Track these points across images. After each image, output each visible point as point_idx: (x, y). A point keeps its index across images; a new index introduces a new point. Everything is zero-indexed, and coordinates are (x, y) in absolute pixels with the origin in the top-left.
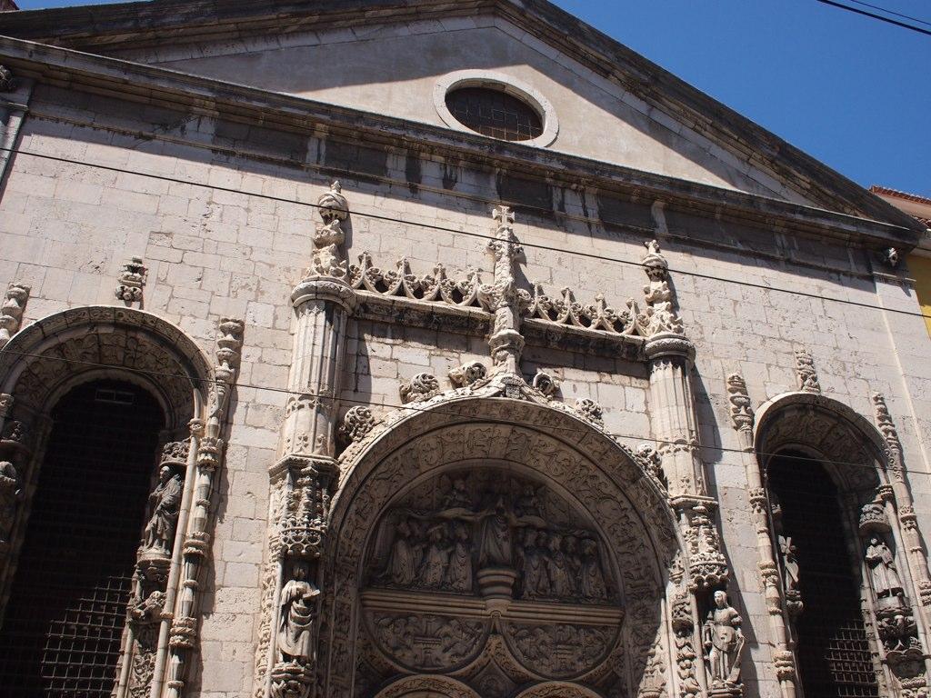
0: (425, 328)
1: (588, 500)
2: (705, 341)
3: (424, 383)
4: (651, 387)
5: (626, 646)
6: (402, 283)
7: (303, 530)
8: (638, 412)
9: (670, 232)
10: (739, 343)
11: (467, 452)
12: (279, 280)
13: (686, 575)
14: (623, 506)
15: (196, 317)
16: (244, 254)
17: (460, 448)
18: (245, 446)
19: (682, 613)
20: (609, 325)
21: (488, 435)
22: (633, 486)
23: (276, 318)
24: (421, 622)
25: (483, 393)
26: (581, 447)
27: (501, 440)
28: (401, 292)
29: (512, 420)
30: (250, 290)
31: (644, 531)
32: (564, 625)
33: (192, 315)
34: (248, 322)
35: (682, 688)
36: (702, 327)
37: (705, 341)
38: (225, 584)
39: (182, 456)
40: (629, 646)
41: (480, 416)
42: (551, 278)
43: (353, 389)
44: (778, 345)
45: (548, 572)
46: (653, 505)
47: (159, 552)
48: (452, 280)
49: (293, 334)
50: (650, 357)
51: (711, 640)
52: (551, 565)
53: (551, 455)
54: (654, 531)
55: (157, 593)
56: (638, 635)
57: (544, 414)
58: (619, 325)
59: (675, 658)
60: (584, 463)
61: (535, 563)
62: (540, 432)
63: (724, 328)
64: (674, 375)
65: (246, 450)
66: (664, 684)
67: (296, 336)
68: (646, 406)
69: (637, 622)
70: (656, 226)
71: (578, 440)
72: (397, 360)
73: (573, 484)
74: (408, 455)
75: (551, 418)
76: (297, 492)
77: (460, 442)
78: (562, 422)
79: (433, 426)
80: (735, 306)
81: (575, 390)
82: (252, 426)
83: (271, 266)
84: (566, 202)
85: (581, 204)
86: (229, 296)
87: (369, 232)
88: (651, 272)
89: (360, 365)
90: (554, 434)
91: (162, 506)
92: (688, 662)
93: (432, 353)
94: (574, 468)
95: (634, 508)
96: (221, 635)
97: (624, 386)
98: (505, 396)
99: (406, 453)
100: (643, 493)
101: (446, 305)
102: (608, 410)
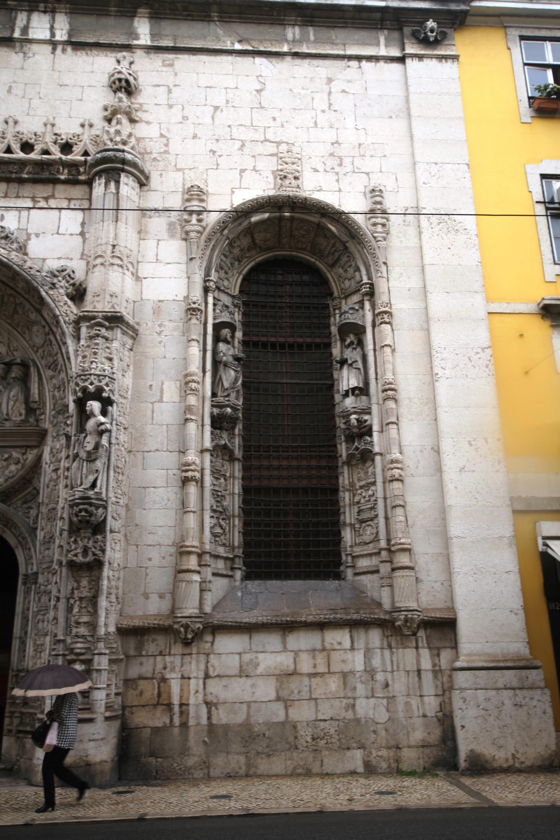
2: (169, 153)
5: (44, 464)
8: (72, 235)
9: (152, 41)
10: (211, 151)
36: (168, 140)
37: (169, 153)
44: (260, 148)
58: (67, 148)
63: (195, 137)
64: (105, 190)
70: (137, 38)
80: (215, 112)
84: (31, 25)
85: (48, 26)
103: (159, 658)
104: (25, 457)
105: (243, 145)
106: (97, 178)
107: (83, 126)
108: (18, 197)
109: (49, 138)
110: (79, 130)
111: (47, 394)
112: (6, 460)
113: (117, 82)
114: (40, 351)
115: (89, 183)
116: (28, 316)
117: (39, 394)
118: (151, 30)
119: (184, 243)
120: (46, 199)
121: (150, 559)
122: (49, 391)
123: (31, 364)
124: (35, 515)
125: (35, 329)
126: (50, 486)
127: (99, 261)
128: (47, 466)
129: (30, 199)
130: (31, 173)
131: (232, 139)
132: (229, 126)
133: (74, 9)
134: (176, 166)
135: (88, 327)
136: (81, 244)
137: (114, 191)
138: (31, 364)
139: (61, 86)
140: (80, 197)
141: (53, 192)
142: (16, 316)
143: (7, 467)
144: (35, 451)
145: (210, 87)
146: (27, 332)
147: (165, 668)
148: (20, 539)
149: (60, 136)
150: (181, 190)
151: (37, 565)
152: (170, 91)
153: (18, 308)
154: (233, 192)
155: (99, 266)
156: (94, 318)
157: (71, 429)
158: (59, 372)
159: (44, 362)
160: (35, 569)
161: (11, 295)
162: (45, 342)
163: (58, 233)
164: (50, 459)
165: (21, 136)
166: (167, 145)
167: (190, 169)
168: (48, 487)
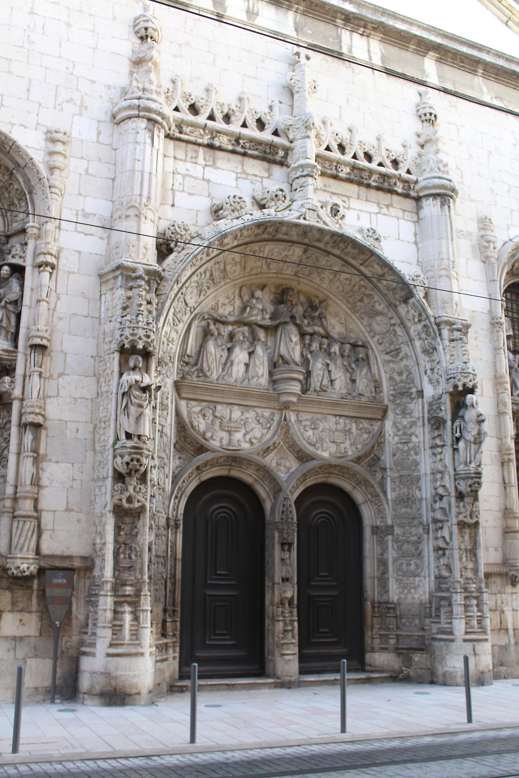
0: (233, 152)
1: (363, 316)
3: (235, 203)
4: (420, 221)
5: (387, 436)
6: (212, 109)
7: (138, 328)
10: (490, 189)
11: (265, 267)
12: (101, 97)
13: (443, 380)
14: (393, 322)
15: (25, 127)
16: (67, 68)
17: (259, 264)
18: (77, 251)
19: (438, 411)
20: (388, 163)
22: (403, 305)
23: (99, 133)
24: (226, 410)
25: (290, 216)
26: (362, 268)
28: (211, 118)
29: (306, 241)
30: (75, 104)
31: (409, 343)
32: (340, 416)
33: (22, 125)
34: (75, 134)
35: (432, 469)
36: (462, 172)
38: (66, 373)
39: (21, 257)
40: (390, 435)
41: (280, 236)
42: (340, 116)
43: (171, 204)
45: (329, 371)
46: (420, 321)
47: (6, 343)
48: (257, 111)
49: (115, 150)
50: (421, 194)
51: (461, 432)
52: (332, 367)
54: (418, 344)
55: (7, 379)
56: (397, 427)
57: (335, 238)
58: (395, 163)
59: (427, 446)
60: (362, 283)
61: (319, 365)
62: (329, 253)
63: (479, 174)
65: (77, 255)
66: (416, 466)
67: (118, 151)
68: (416, 237)
69: (398, 416)
71: (361, 262)
72: (209, 181)
73: (351, 300)
75: (341, 241)
76: (130, 294)
81: (358, 218)
82: (82, 233)
83: (93, 82)
84: (353, 45)
86: (55, 108)
87: (181, 56)
88: (423, 118)
89: (175, 180)
90: (342, 255)
91: (6, 302)
92: (439, 450)
93: (239, 175)
95: (402, 324)
96: (66, 416)
97: (398, 219)
98: (305, 219)
100: (412, 312)
101: (253, 132)
102: (385, 238)
103: (498, 596)
104: (373, 428)
105: (509, 190)
106: (431, 199)
107: (404, 146)
108: (367, 200)
109: (384, 153)
110: (401, 150)
111: (383, 375)
112: (361, 429)
113: (428, 115)
114: (377, 337)
115: (418, 199)
116: (373, 306)
118: (438, 73)
119: (482, 264)
120: (388, 206)
121: (487, 521)
122: (385, 372)
124: (380, 477)
125: (379, 318)
126: (398, 455)
127: (443, 272)
128: (391, 438)
129: (375, 205)
130: (376, 182)
131: (502, 182)
132: (500, 170)
133: (384, 39)
134: (469, 196)
135: (449, 330)
136: (416, 252)
137: (448, 214)
139: (384, 106)
140: (410, 210)
141: (392, 202)
142: (359, 304)
143: (361, 435)
144: (379, 423)
145: (484, 133)
146: (366, 319)
147: (502, 603)
148: (369, 496)
149: (391, 152)
150: (476, 218)
151: (392, 520)
152: (458, 131)
153: (365, 298)
154: (509, 228)
155: (444, 277)
156: (453, 324)
157: (446, 414)
158: (402, 360)
159: (381, 348)
160: (390, 522)
161: (363, 286)
162: (388, 331)
163: (399, 239)
164: (394, 433)
165: (363, 146)
166: (462, 177)
167: (479, 202)
168: (394, 455)
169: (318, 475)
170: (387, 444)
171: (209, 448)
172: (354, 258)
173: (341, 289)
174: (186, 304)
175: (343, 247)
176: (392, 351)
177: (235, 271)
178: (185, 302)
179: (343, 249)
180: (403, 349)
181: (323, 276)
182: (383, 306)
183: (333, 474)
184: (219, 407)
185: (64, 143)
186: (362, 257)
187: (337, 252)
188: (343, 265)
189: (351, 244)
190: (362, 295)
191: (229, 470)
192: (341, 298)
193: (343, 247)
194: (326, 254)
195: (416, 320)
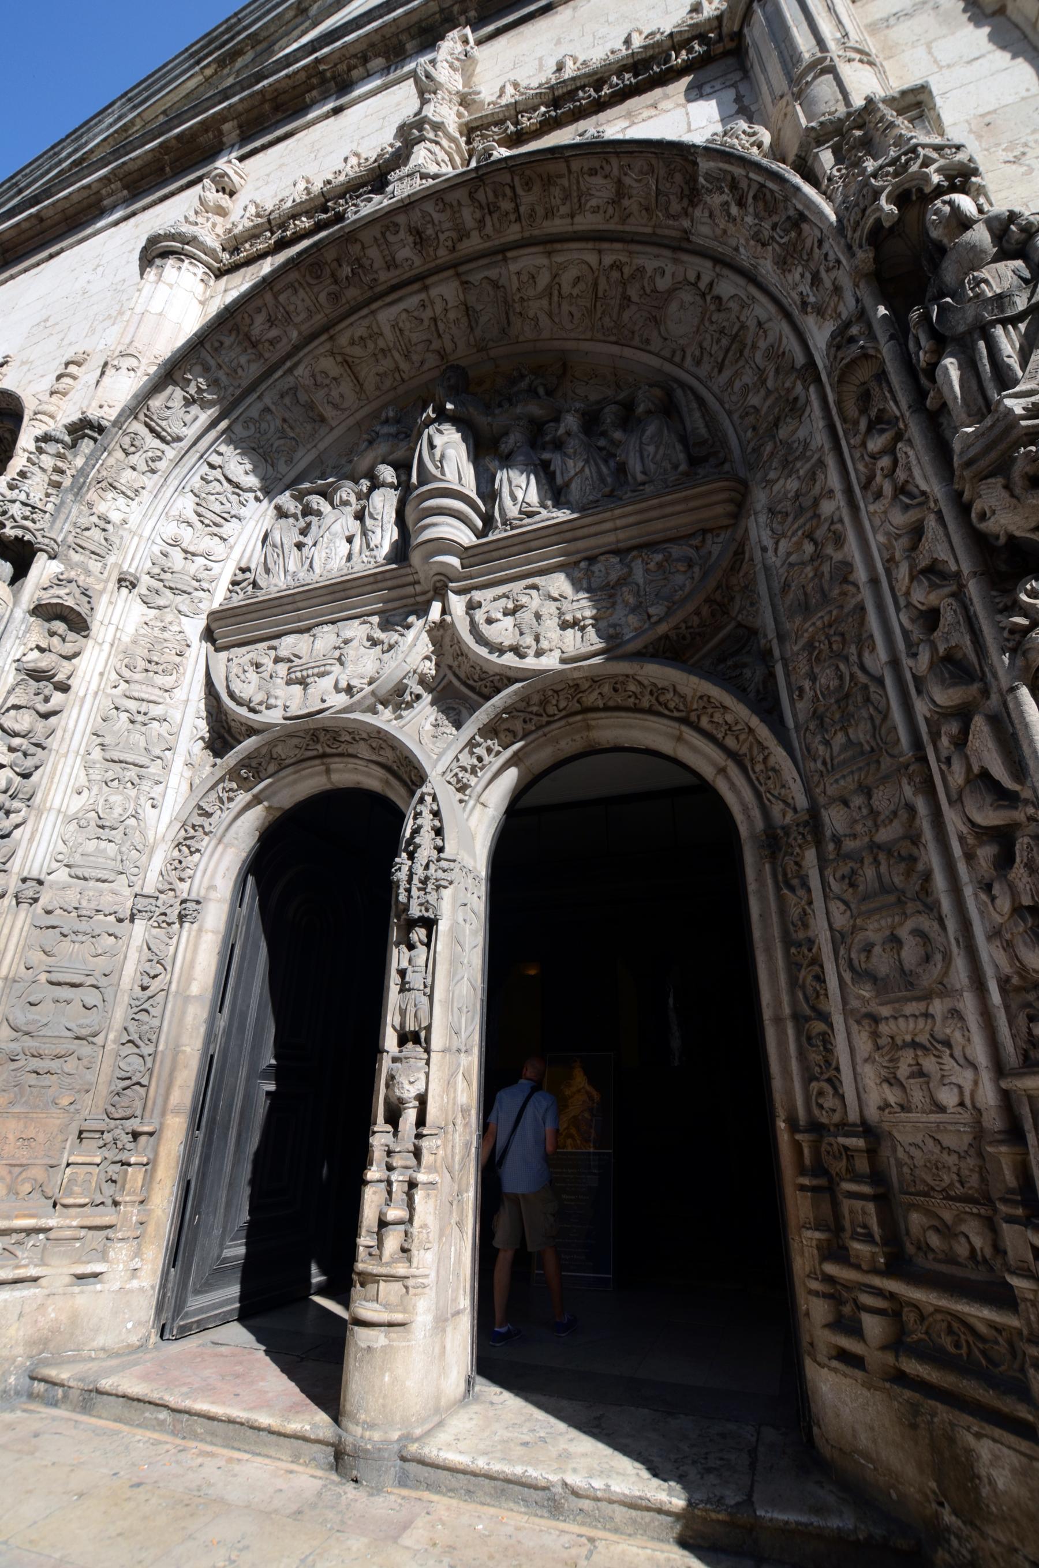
5: (758, 554)
21: (426, 315)
27: (452, 315)
29: (443, 255)
32: (592, 560)
41: (386, 277)
53: (548, 293)
60: (608, 260)
62: (502, 252)
73: (607, 320)
74: (287, 400)
77: (382, 350)
78: (520, 191)
79: (307, 328)
94: (596, 284)
99: (282, 397)
111: (727, 423)
116: (655, 291)
117: (707, 426)
122: (729, 413)
123: (675, 386)
138: (675, 386)
169: (548, 723)
170: (761, 578)
171: (256, 726)
172: (550, 213)
173: (577, 315)
174: (237, 486)
175: (513, 205)
176: (727, 351)
177: (342, 396)
178: (229, 481)
179: (517, 209)
180: (748, 323)
181: (531, 314)
182: (670, 269)
183: (595, 709)
184: (288, 640)
185: (79, 364)
186: (557, 192)
187: (513, 232)
188: (549, 254)
189: (517, 179)
190: (620, 289)
191: (328, 771)
192: (589, 335)
193: (513, 205)
194: (500, 257)
195: (734, 210)
